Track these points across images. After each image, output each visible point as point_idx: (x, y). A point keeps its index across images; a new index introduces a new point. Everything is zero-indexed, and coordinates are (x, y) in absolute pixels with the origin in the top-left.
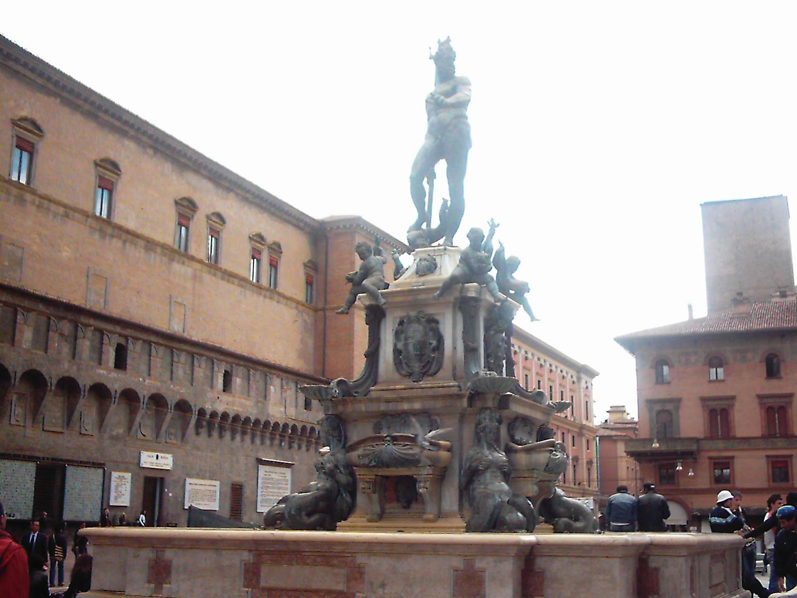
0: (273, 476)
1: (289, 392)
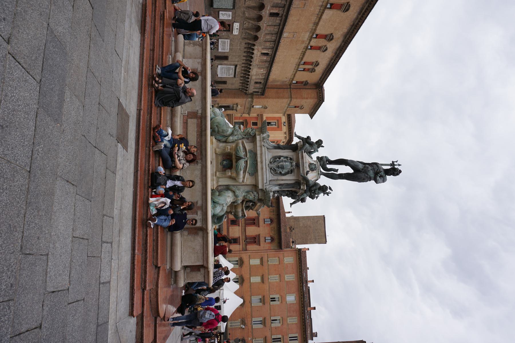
0: (231, 71)
1: (261, 76)
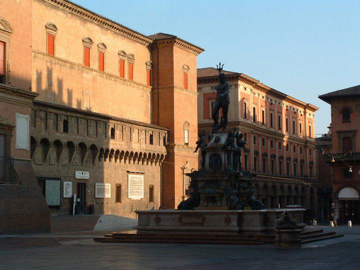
0: (135, 179)
